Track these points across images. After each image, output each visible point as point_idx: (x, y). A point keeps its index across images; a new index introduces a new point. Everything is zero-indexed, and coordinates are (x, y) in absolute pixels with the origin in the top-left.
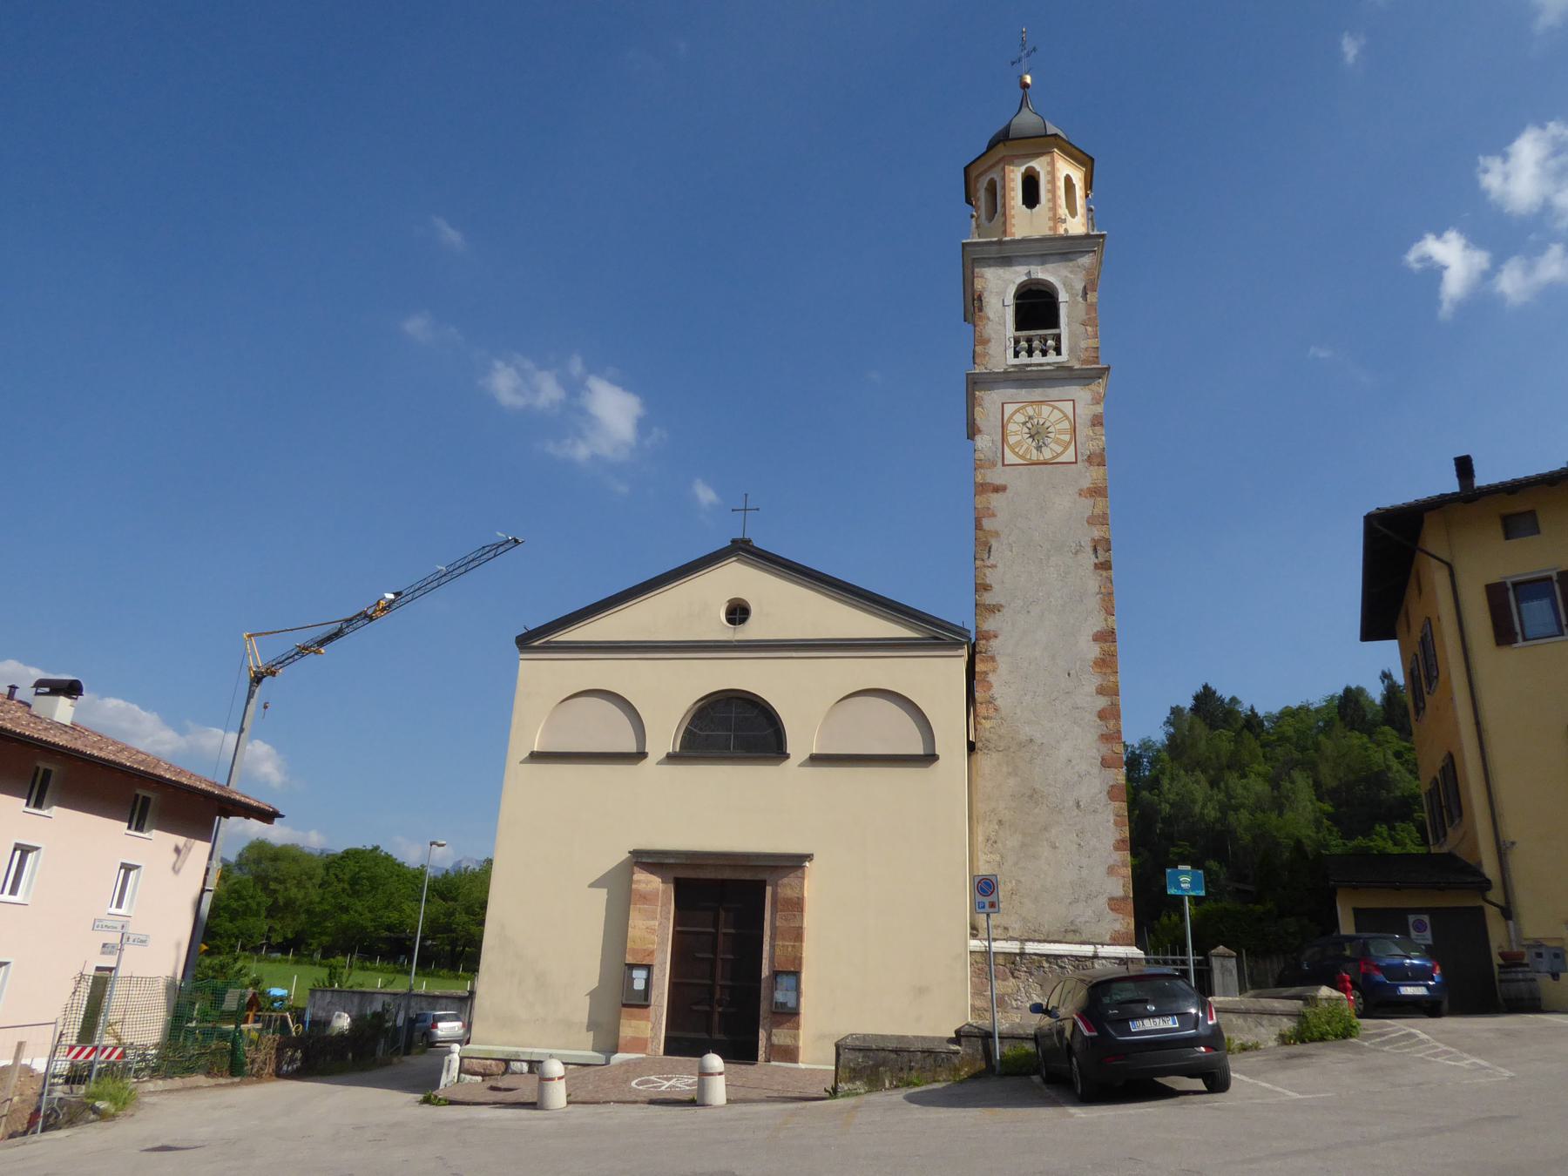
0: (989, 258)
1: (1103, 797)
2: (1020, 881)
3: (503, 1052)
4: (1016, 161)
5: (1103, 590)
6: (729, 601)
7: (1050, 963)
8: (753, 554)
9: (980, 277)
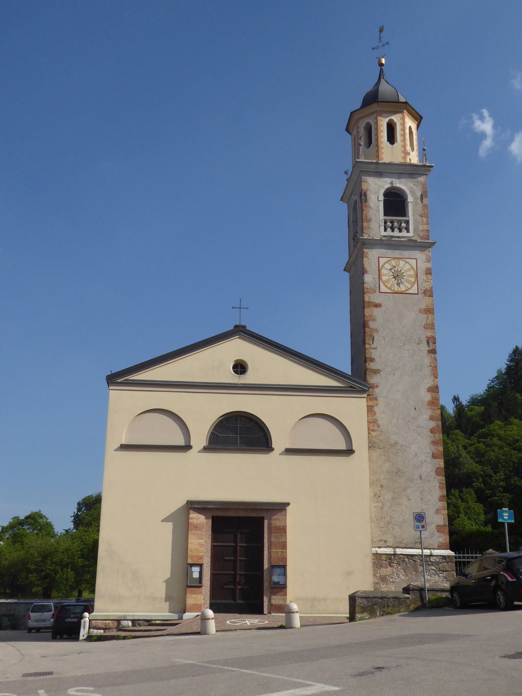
0: (370, 171)
1: (433, 474)
2: (392, 517)
3: (116, 616)
4: (383, 114)
5: (432, 365)
6: (235, 361)
7: (409, 559)
8: (248, 334)
9: (365, 182)
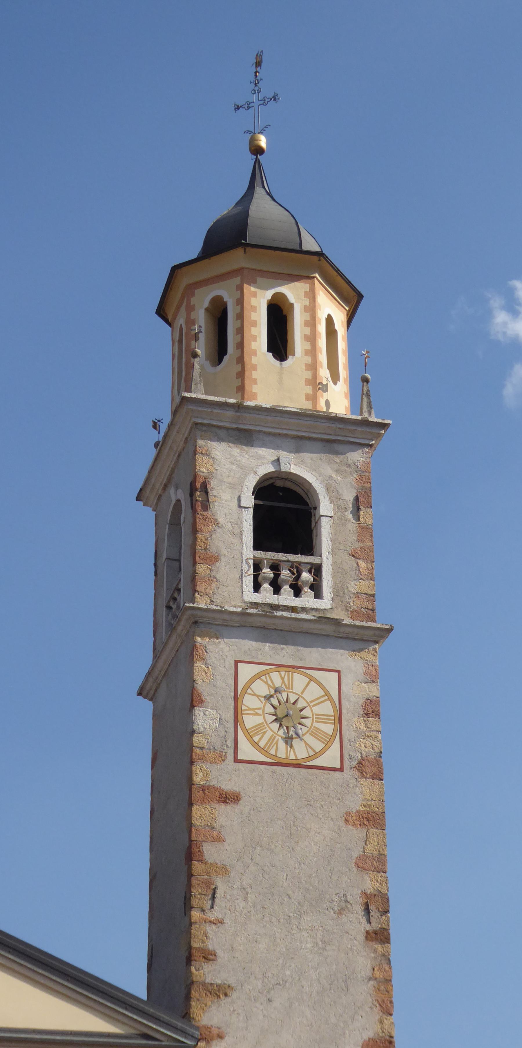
0: (219, 427)
4: (259, 280)
5: (378, 974)
